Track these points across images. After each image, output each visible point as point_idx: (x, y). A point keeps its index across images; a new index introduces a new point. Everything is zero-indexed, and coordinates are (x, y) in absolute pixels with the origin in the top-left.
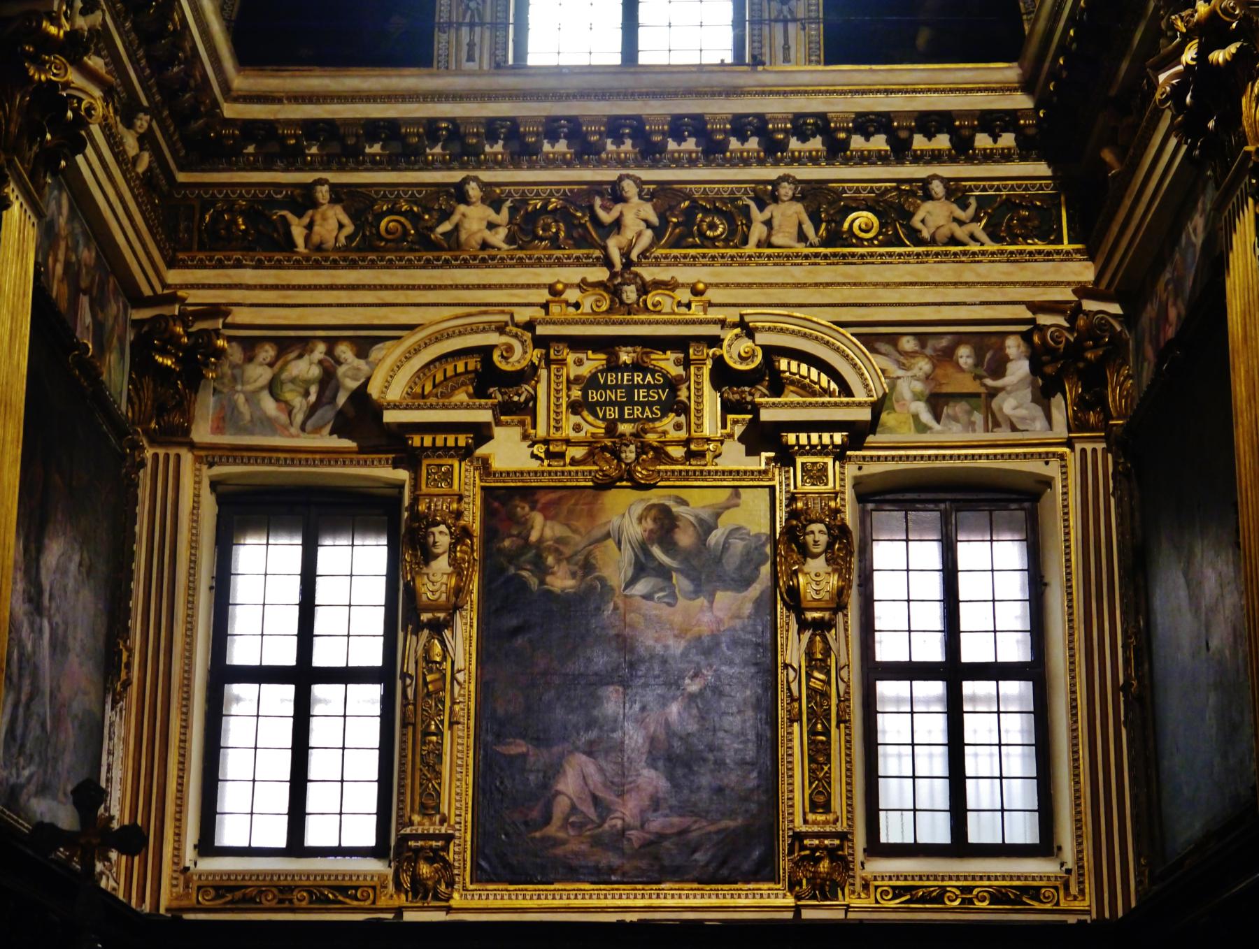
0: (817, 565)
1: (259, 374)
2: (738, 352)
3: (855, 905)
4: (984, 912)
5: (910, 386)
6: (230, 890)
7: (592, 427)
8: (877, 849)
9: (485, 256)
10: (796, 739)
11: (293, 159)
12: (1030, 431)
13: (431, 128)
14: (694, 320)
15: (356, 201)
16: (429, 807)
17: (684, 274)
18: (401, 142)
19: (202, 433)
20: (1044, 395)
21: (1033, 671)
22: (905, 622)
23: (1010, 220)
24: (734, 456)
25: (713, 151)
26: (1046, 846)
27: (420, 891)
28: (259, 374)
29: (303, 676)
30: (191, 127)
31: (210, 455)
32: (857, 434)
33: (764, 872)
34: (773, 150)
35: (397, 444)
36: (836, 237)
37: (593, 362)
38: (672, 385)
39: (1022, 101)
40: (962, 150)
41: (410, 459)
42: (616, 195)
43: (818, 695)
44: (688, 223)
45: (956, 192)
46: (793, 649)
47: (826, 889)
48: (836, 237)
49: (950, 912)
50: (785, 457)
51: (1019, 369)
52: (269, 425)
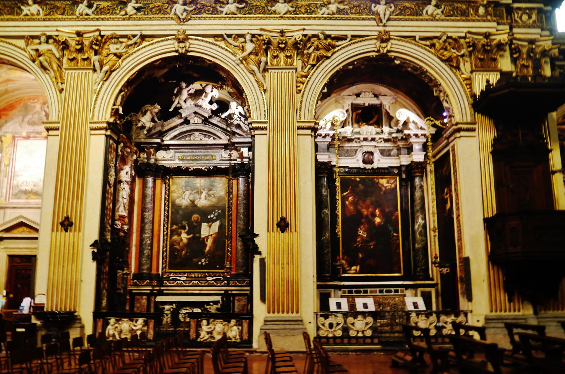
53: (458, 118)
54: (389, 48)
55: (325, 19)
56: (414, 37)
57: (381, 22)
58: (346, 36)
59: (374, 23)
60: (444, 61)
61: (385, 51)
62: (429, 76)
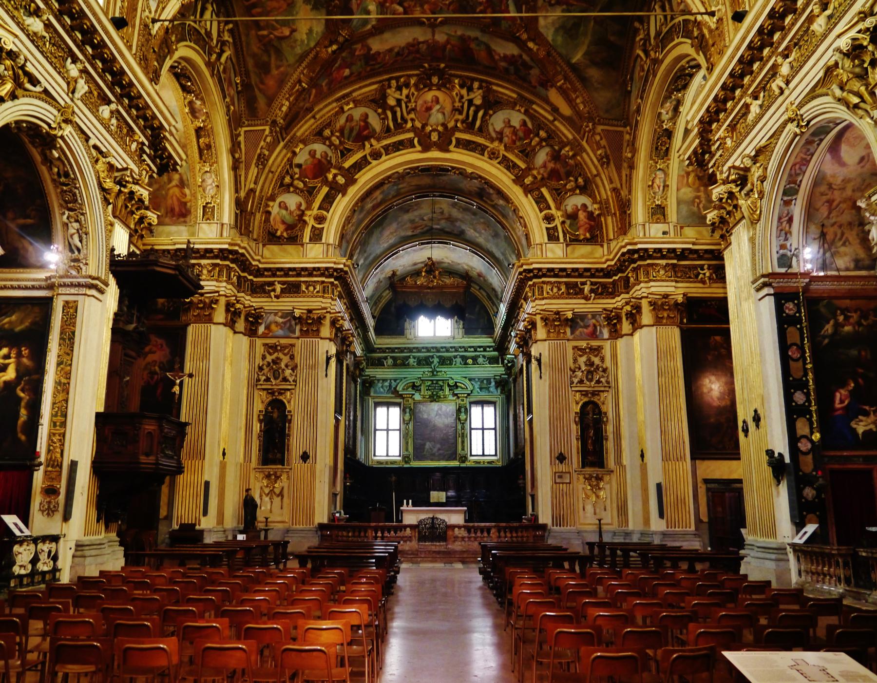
0: (463, 414)
1: (380, 385)
2: (451, 383)
3: (468, 464)
4: (486, 465)
5: (477, 386)
6: (379, 462)
7: (430, 393)
8: (471, 455)
9: (413, 367)
10: (460, 440)
11: (384, 352)
12: (496, 394)
13: (405, 348)
14: (445, 377)
15: (394, 359)
16: (407, 450)
17: (443, 370)
18: (401, 350)
19: (372, 394)
20: (497, 388)
21: (495, 429)
22: (476, 422)
23: (492, 361)
24: (451, 397)
25: (447, 351)
26: (496, 455)
27: (406, 462)
28: (380, 385)
29: (388, 430)
30: (368, 347)
31: (374, 398)
32: (469, 395)
33: (455, 459)
34: (456, 351)
35: (401, 396)
36: (466, 364)
37: (430, 383)
38: (441, 386)
39: (493, 344)
40: (485, 350)
41: (403, 398)
42: (432, 357)
43: (463, 434)
44: (444, 361)
45: (484, 357)
46: (459, 427)
47: (463, 462)
48: (466, 364)
49: (481, 465)
50: (458, 398)
51: (493, 384)
52: (381, 393)
53: (92, 270)
54: (65, 134)
55: (28, 36)
56: (89, 138)
57: (73, 92)
58: (39, 82)
59: (65, 86)
60: (103, 189)
61: (59, 134)
62: (74, 195)
